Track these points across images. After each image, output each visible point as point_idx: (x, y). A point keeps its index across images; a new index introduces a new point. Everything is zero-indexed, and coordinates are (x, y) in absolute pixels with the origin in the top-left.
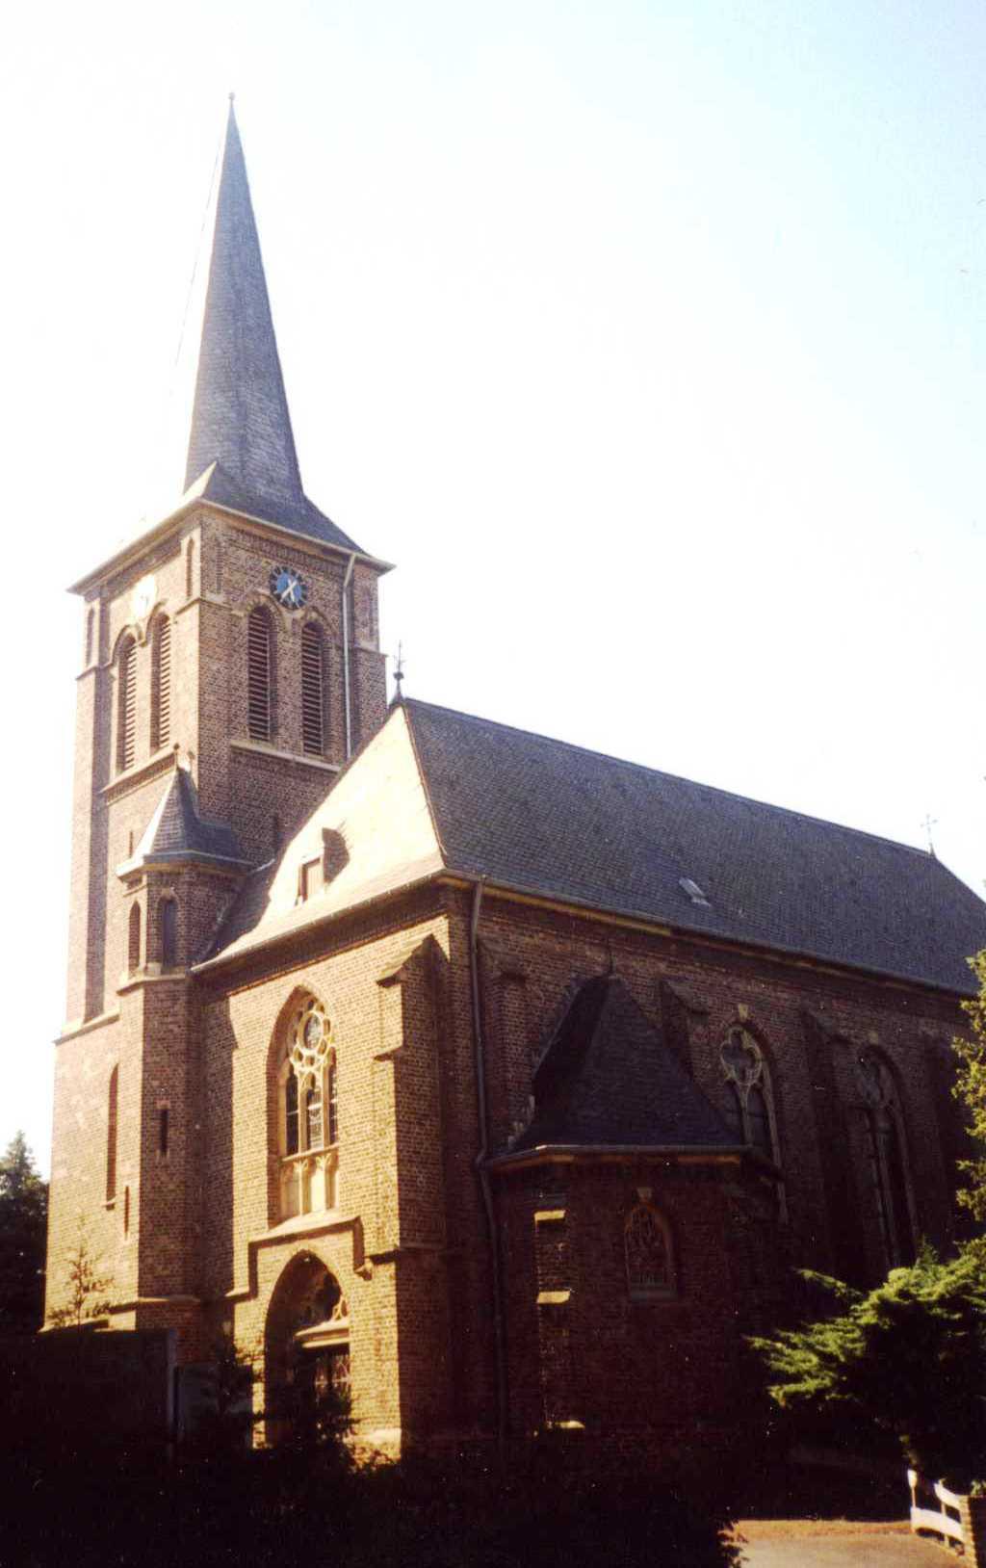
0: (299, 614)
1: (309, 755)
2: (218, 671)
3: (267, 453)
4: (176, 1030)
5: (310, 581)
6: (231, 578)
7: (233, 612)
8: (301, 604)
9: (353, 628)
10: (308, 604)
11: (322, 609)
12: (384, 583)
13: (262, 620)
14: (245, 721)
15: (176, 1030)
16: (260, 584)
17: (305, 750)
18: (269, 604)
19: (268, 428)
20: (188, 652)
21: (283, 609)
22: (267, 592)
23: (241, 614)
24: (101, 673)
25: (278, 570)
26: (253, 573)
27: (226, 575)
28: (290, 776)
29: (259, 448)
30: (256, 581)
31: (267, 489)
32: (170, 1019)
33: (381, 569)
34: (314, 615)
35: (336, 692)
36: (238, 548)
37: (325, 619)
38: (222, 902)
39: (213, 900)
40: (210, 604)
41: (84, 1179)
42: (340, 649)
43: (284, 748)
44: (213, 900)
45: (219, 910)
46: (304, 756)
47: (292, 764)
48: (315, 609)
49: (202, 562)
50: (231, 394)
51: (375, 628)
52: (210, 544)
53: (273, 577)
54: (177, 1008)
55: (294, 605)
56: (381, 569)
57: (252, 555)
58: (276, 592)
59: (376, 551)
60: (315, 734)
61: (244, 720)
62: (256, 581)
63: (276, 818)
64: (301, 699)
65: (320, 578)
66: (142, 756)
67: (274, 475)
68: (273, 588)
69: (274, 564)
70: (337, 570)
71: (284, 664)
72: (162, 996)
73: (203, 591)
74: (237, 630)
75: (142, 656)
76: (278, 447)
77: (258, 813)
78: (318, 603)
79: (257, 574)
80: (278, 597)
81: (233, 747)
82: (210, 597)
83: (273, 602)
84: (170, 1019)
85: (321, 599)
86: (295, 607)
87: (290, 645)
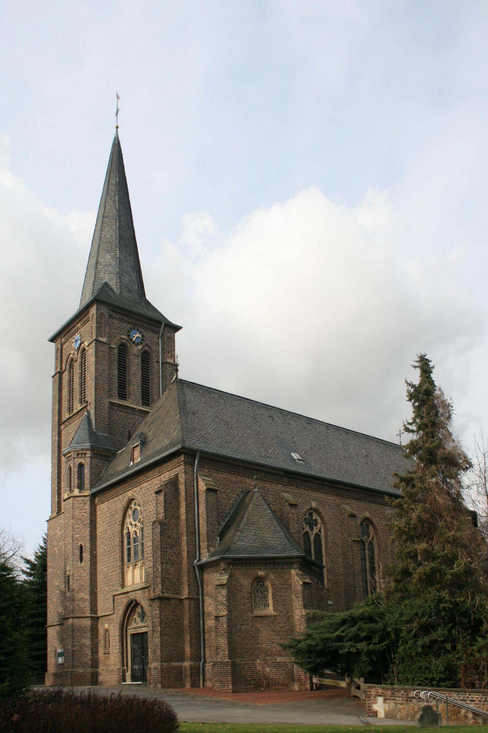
0: (140, 347)
1: (144, 406)
2: (104, 370)
3: (128, 279)
4: (86, 515)
5: (145, 333)
6: (110, 331)
7: (110, 346)
8: (141, 343)
9: (163, 353)
10: (144, 344)
11: (150, 345)
12: (178, 335)
13: (123, 349)
14: (116, 392)
15: (86, 515)
16: (123, 334)
17: (142, 405)
18: (127, 343)
19: (129, 269)
20: (91, 363)
21: (133, 345)
22: (126, 338)
23: (114, 347)
24: (60, 374)
25: (131, 329)
26: (120, 329)
27: (108, 330)
28: (135, 415)
29: (124, 277)
30: (122, 332)
31: (128, 294)
32: (83, 511)
33: (177, 328)
34: (147, 348)
35: (156, 381)
36: (113, 319)
37: (151, 349)
38: (104, 465)
39: (100, 464)
40: (100, 342)
41: (58, 572)
42: (158, 362)
43: (133, 403)
44: (100, 464)
45: (104, 468)
46: (142, 407)
47: (136, 410)
48: (147, 345)
49: (97, 324)
50: (113, 254)
51: (173, 354)
52: (100, 316)
53: (129, 331)
54: (86, 507)
55: (138, 343)
56: (177, 328)
57: (119, 322)
58: (130, 338)
59: (174, 320)
60: (146, 399)
61: (116, 392)
62: (122, 332)
63: (129, 432)
64: (141, 383)
65: (150, 332)
66: (77, 406)
67: (131, 288)
68: (129, 336)
69: (129, 326)
70: (157, 329)
71: (133, 368)
72: (80, 502)
73: (97, 336)
74: (113, 353)
75: (77, 365)
76: (134, 277)
77: (121, 429)
78: (149, 343)
79: (122, 330)
80: (131, 340)
81: (110, 402)
82: (101, 339)
83: (128, 342)
84: (83, 511)
85: (150, 341)
86: (138, 344)
87: (136, 360)
